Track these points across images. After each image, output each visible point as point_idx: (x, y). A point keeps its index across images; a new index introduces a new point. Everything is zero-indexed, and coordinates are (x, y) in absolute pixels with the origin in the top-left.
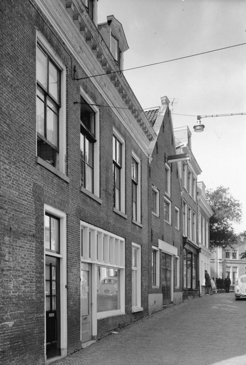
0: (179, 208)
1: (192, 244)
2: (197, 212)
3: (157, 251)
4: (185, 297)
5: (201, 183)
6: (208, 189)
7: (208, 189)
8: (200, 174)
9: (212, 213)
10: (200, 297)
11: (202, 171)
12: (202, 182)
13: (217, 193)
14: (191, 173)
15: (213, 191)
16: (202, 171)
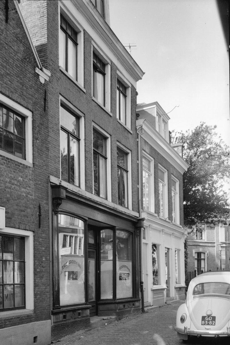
0: (30, 110)
1: (108, 207)
2: (134, 148)
3: (26, 239)
4: (58, 331)
5: (155, 106)
6: (182, 131)
7: (182, 131)
8: (141, 79)
9: (185, 167)
10: (143, 311)
11: (144, 73)
12: (156, 103)
13: (197, 134)
14: (108, 64)
15: (191, 134)
16: (144, 73)
